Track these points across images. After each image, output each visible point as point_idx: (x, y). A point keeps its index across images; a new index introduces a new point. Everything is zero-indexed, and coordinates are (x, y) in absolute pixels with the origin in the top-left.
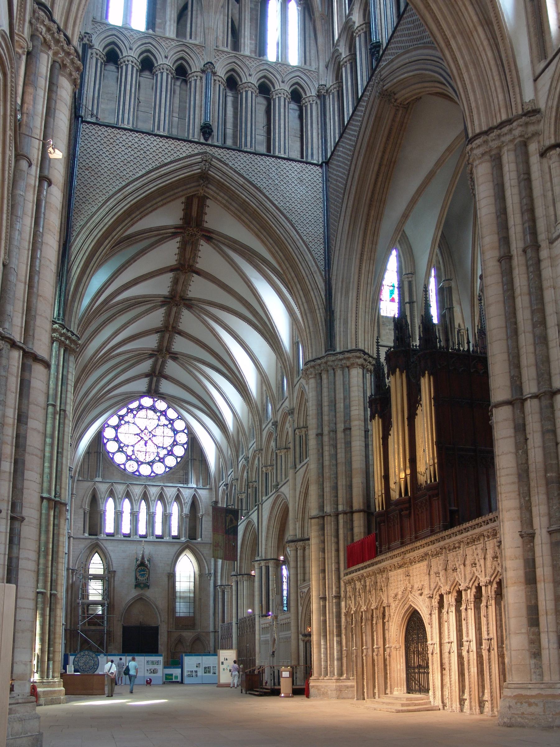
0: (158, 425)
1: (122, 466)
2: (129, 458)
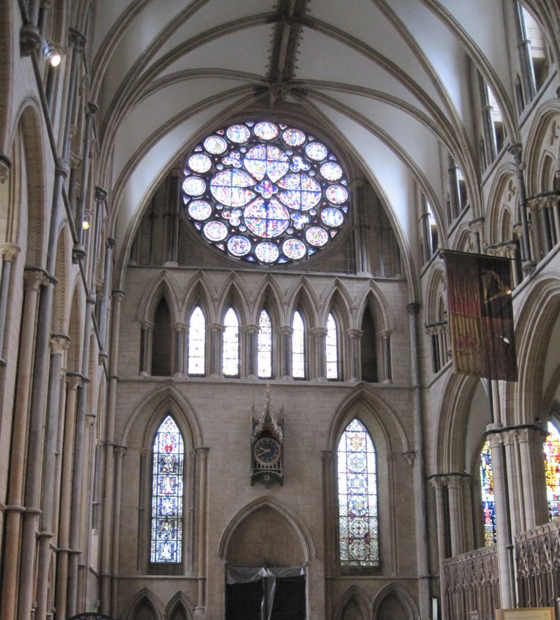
0: (289, 173)
1: (221, 247)
2: (233, 232)
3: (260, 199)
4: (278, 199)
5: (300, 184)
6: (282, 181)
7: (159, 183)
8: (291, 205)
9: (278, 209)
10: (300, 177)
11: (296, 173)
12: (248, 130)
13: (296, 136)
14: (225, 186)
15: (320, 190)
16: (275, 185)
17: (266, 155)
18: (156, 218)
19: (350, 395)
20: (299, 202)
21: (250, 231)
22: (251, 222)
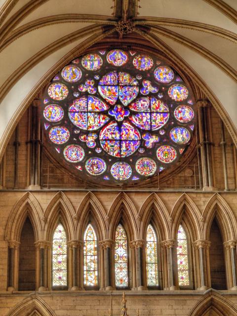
2: (90, 154)
3: (114, 122)
4: (131, 122)
5: (150, 107)
6: (133, 104)
7: (21, 115)
8: (142, 126)
9: (131, 131)
10: (150, 100)
11: (146, 96)
12: (100, 58)
13: (144, 61)
14: (81, 112)
15: (168, 111)
16: (126, 108)
17: (118, 81)
18: (19, 145)
19: (201, 302)
20: (149, 122)
21: (105, 152)
22: (106, 144)
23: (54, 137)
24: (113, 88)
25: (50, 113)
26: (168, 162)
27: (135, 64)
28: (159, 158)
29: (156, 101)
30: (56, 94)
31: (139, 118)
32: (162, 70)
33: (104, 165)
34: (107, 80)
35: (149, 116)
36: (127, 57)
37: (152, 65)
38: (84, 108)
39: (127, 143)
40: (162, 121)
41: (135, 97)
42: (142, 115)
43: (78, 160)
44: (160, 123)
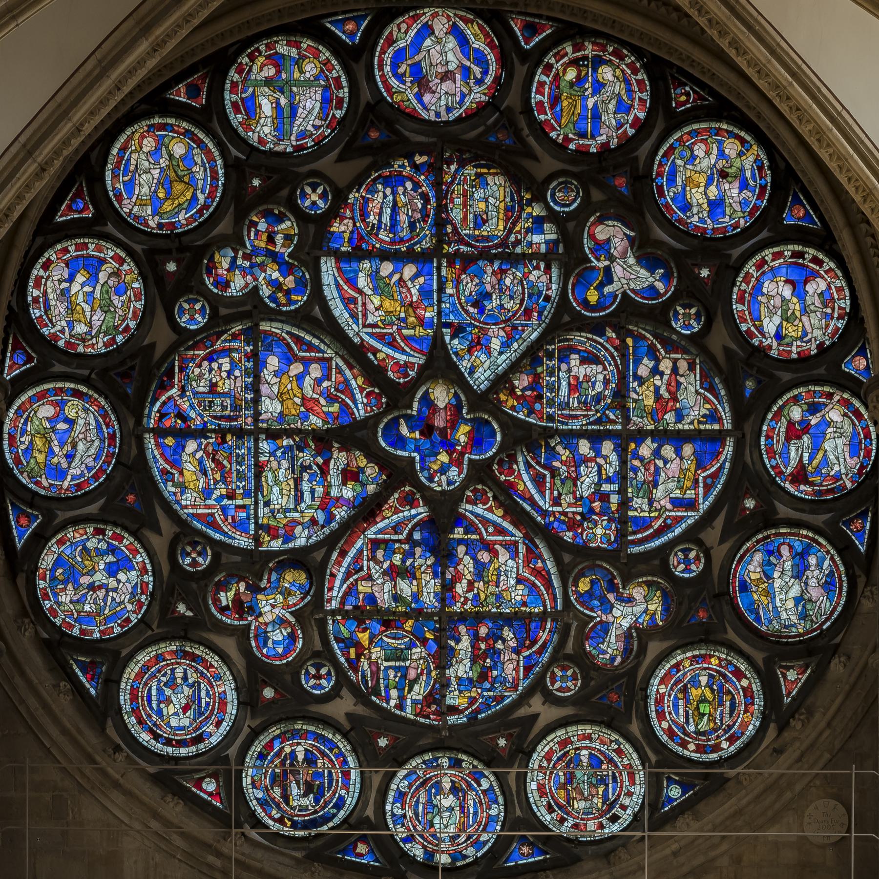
5: (621, 394)
6: (522, 381)
8: (572, 525)
9: (504, 556)
10: (622, 349)
11: (597, 327)
12: (337, 70)
13: (599, 87)
14: (222, 433)
15: (728, 425)
17: (441, 223)
20: (614, 499)
21: (354, 689)
22: (364, 637)
23: (64, 598)
24: (409, 271)
25: (39, 443)
26: (714, 756)
27: (540, 104)
28: (660, 728)
29: (658, 361)
30: (71, 309)
31: (554, 472)
32: (699, 150)
33: (346, 775)
34: (372, 219)
35: (614, 457)
36: (491, 57)
37: (642, 115)
38: (236, 407)
39: (483, 631)
40: (690, 494)
41: (534, 336)
42: (574, 449)
43: (199, 739)
44: (677, 503)
